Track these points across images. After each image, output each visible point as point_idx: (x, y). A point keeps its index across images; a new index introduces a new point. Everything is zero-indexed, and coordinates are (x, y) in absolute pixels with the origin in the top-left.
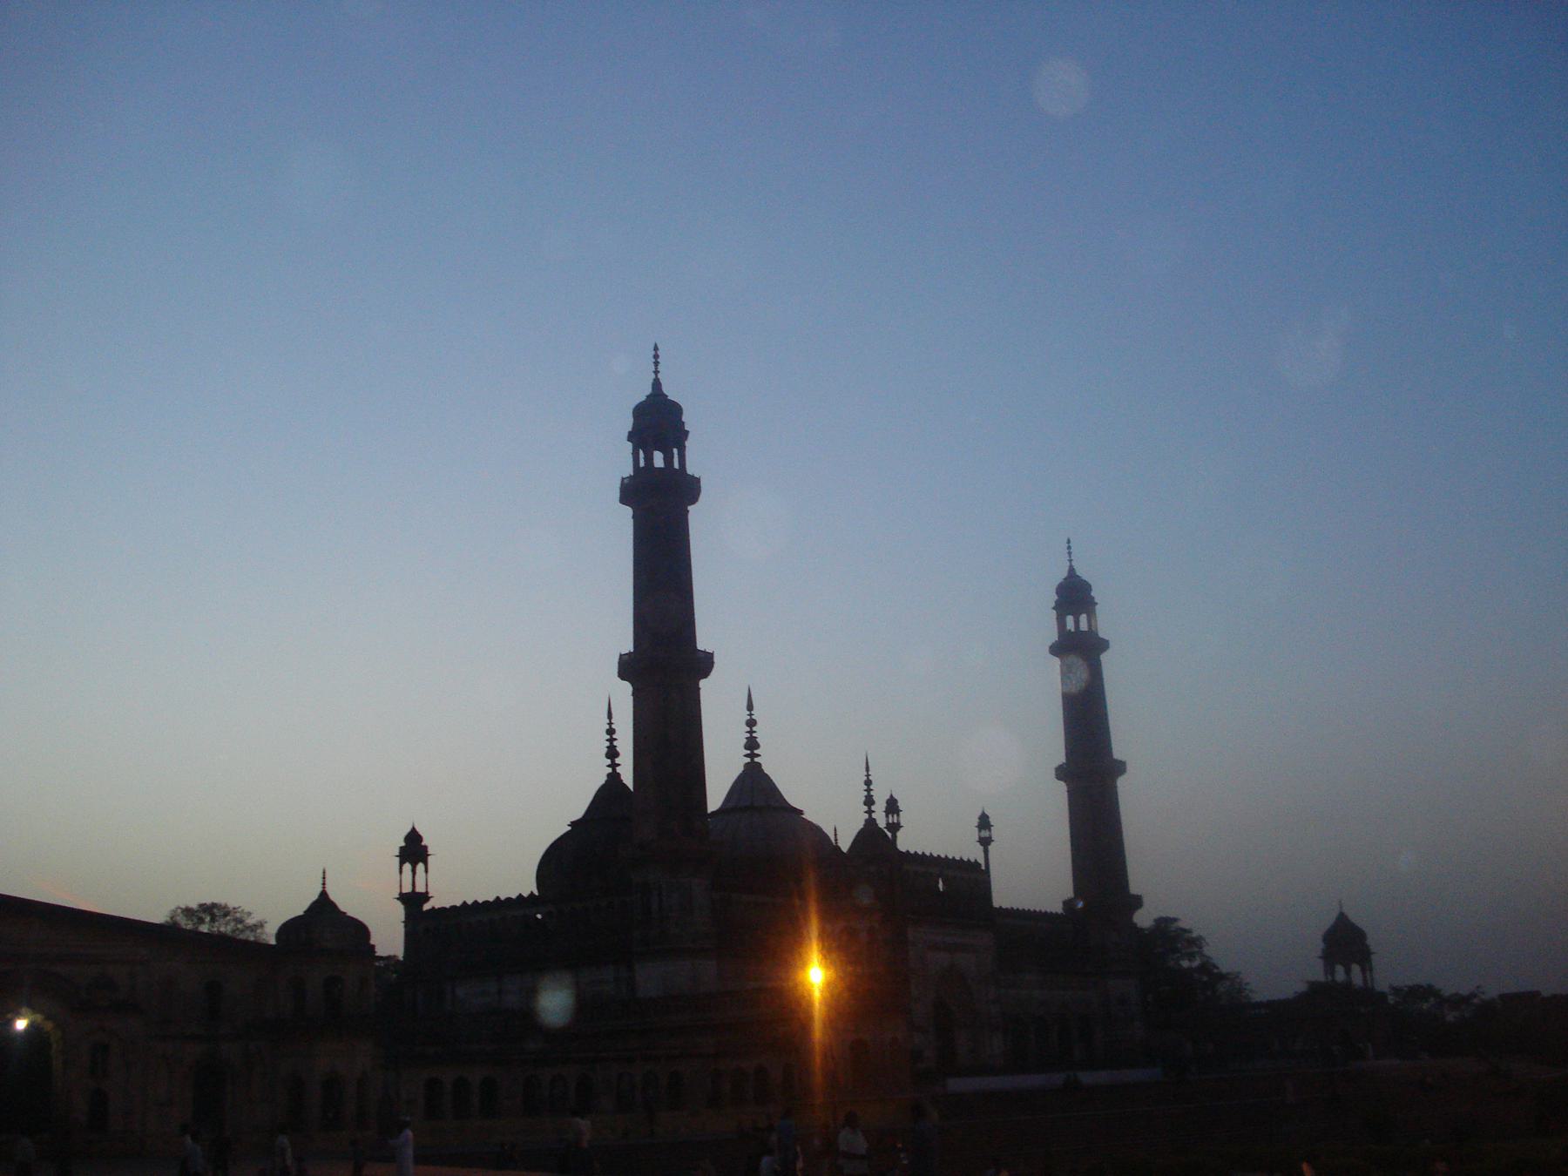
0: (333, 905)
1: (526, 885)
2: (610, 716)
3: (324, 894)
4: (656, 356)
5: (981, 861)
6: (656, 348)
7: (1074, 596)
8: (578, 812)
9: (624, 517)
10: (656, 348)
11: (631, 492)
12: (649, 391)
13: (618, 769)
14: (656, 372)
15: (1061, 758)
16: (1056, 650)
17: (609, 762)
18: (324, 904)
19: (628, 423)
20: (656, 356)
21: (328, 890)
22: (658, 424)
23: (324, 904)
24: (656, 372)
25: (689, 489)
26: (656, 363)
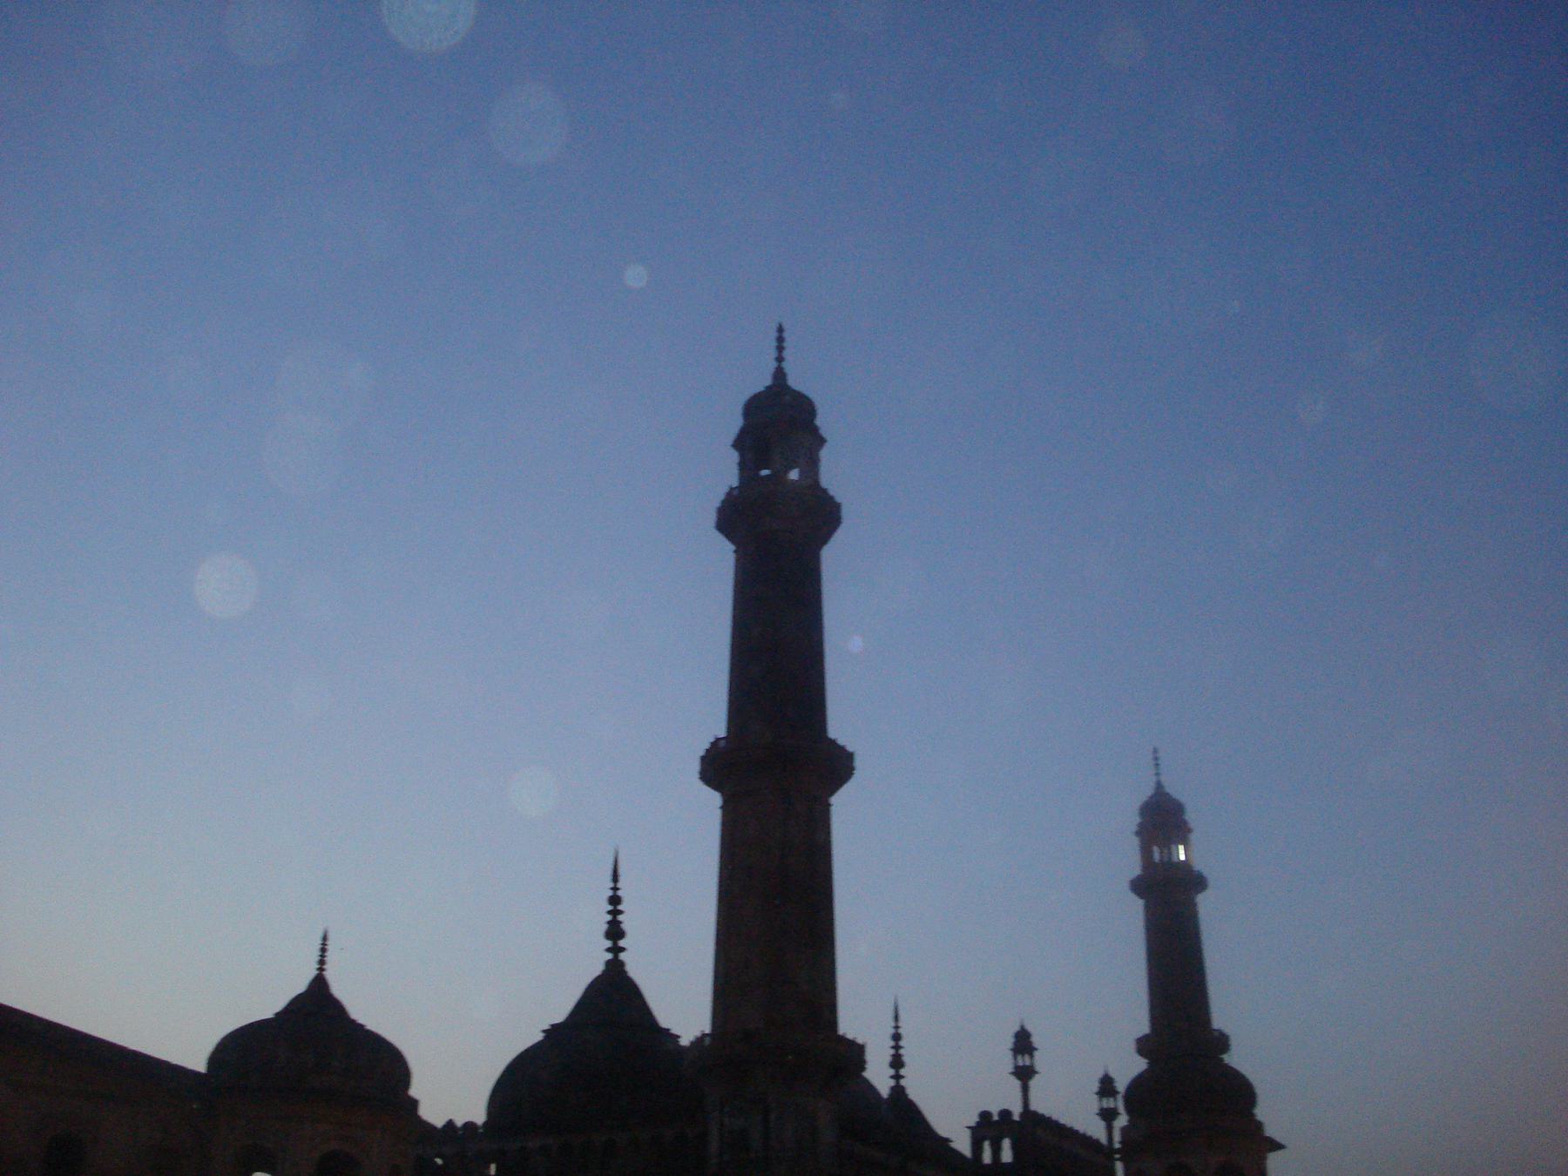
1: (479, 1116)
2: (615, 878)
3: (320, 984)
4: (780, 339)
6: (780, 330)
7: (1162, 819)
8: (560, 1010)
9: (721, 557)
10: (780, 330)
11: (734, 517)
12: (768, 382)
13: (622, 956)
14: (780, 359)
15: (1143, 1027)
17: (609, 944)
18: (317, 1007)
19: (736, 423)
20: (780, 339)
21: (330, 975)
22: (778, 427)
23: (317, 1007)
24: (780, 359)
25: (822, 516)
26: (780, 349)
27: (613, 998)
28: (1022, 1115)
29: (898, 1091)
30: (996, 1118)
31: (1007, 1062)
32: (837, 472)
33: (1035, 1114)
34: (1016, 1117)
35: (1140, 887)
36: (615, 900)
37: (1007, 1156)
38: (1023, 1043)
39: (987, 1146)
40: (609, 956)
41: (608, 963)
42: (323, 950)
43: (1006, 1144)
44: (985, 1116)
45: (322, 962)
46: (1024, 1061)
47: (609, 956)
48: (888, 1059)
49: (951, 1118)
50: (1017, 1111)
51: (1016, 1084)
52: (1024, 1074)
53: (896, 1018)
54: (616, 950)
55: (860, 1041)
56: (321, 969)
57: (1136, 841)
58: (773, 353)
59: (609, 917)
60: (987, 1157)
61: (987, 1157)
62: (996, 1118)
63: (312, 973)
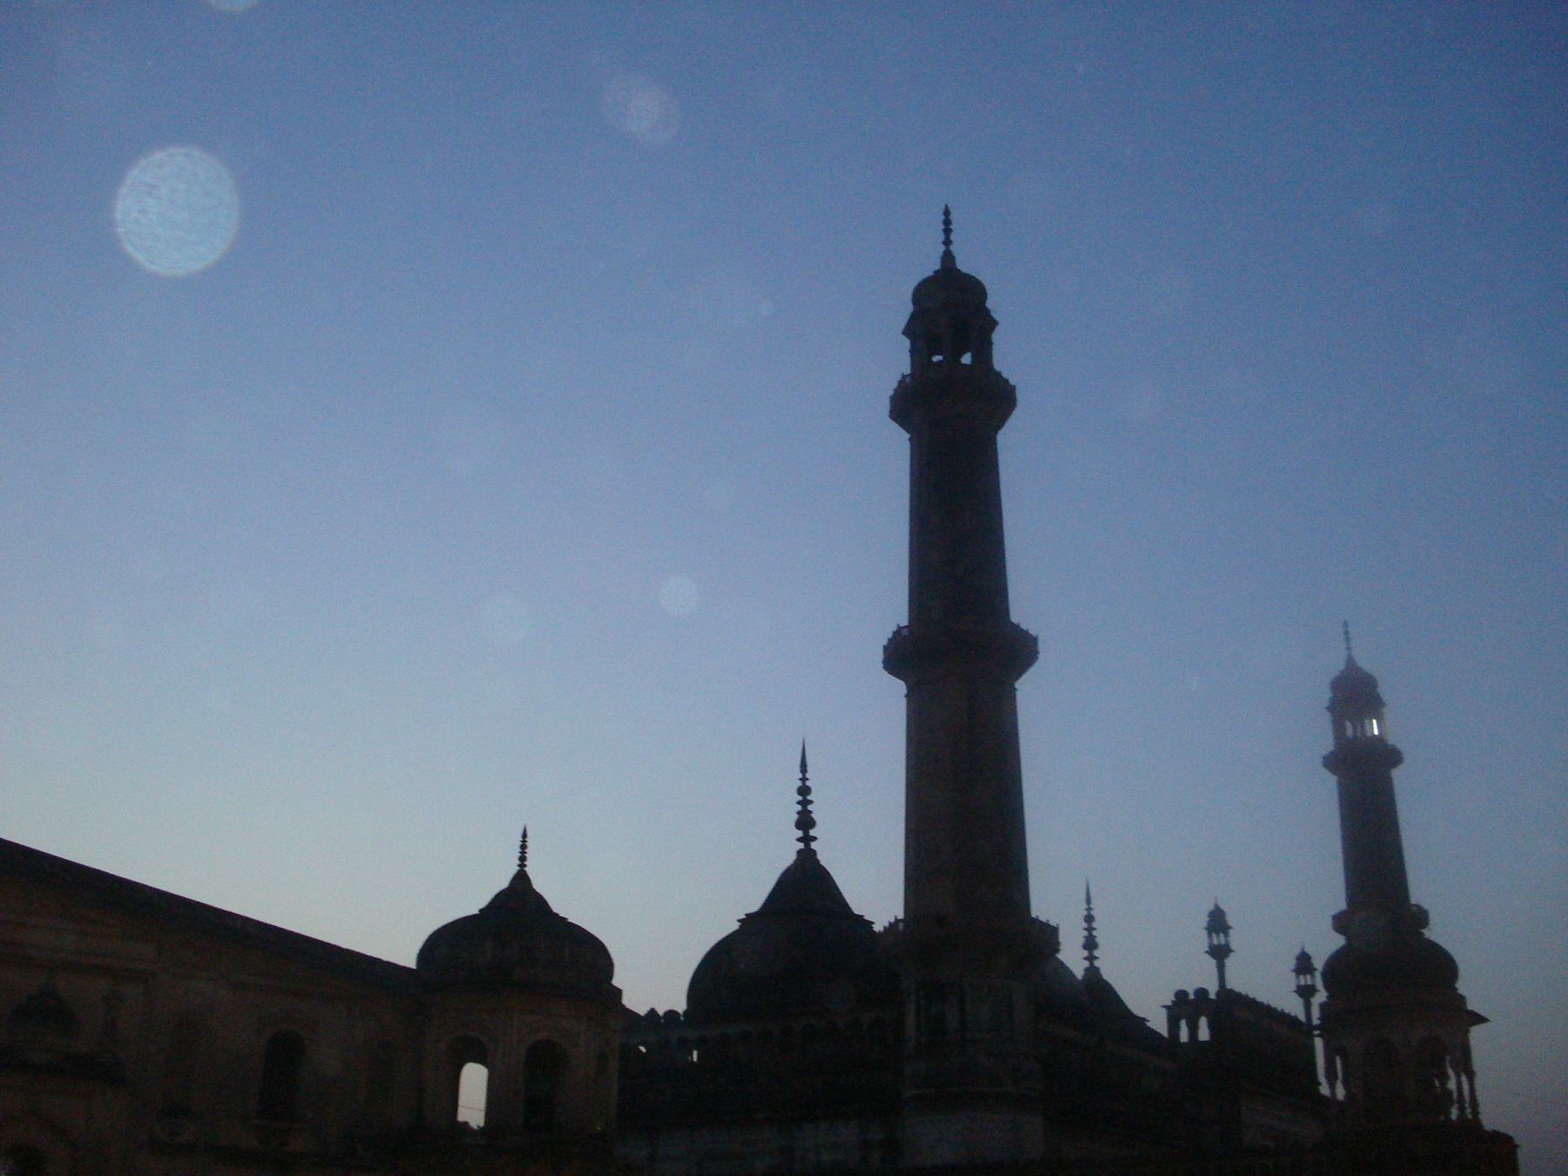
0: (541, 902)
3: (521, 879)
5: (1302, 1018)
6: (947, 212)
7: (1355, 695)
9: (896, 446)
10: (947, 212)
11: (908, 405)
12: (935, 265)
13: (814, 845)
14: (947, 242)
15: (1341, 904)
16: (1331, 762)
17: (800, 834)
18: (519, 904)
19: (903, 310)
21: (530, 870)
22: (950, 315)
23: (519, 904)
24: (947, 242)
25: (997, 399)
26: (947, 231)
27: (806, 889)
28: (1217, 994)
29: (1093, 972)
30: (1192, 997)
31: (1202, 941)
32: (1010, 354)
33: (1231, 991)
34: (1212, 996)
35: (1331, 762)
36: (804, 791)
37: (1204, 1034)
38: (1218, 922)
39: (1183, 1024)
40: (801, 846)
41: (799, 852)
42: (524, 847)
43: (1203, 1022)
44: (1181, 995)
45: (523, 859)
46: (1219, 939)
47: (801, 846)
48: (1082, 941)
49: (1147, 1000)
50: (1213, 989)
51: (1212, 963)
52: (1220, 953)
53: (1088, 901)
54: (807, 839)
55: (1053, 923)
56: (522, 865)
57: (1328, 716)
58: (942, 237)
59: (799, 808)
60: (1184, 1036)
61: (1184, 1036)
62: (1192, 997)
63: (515, 869)
